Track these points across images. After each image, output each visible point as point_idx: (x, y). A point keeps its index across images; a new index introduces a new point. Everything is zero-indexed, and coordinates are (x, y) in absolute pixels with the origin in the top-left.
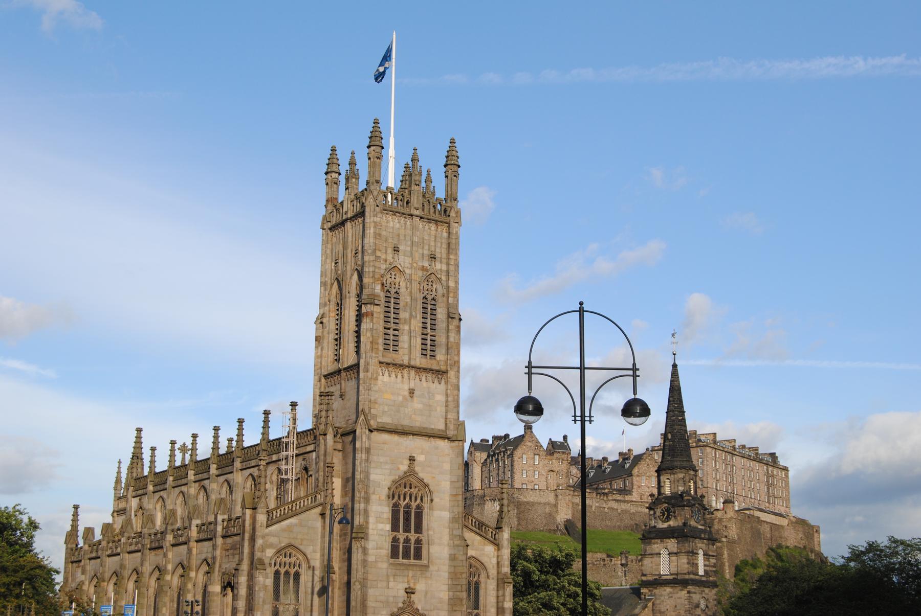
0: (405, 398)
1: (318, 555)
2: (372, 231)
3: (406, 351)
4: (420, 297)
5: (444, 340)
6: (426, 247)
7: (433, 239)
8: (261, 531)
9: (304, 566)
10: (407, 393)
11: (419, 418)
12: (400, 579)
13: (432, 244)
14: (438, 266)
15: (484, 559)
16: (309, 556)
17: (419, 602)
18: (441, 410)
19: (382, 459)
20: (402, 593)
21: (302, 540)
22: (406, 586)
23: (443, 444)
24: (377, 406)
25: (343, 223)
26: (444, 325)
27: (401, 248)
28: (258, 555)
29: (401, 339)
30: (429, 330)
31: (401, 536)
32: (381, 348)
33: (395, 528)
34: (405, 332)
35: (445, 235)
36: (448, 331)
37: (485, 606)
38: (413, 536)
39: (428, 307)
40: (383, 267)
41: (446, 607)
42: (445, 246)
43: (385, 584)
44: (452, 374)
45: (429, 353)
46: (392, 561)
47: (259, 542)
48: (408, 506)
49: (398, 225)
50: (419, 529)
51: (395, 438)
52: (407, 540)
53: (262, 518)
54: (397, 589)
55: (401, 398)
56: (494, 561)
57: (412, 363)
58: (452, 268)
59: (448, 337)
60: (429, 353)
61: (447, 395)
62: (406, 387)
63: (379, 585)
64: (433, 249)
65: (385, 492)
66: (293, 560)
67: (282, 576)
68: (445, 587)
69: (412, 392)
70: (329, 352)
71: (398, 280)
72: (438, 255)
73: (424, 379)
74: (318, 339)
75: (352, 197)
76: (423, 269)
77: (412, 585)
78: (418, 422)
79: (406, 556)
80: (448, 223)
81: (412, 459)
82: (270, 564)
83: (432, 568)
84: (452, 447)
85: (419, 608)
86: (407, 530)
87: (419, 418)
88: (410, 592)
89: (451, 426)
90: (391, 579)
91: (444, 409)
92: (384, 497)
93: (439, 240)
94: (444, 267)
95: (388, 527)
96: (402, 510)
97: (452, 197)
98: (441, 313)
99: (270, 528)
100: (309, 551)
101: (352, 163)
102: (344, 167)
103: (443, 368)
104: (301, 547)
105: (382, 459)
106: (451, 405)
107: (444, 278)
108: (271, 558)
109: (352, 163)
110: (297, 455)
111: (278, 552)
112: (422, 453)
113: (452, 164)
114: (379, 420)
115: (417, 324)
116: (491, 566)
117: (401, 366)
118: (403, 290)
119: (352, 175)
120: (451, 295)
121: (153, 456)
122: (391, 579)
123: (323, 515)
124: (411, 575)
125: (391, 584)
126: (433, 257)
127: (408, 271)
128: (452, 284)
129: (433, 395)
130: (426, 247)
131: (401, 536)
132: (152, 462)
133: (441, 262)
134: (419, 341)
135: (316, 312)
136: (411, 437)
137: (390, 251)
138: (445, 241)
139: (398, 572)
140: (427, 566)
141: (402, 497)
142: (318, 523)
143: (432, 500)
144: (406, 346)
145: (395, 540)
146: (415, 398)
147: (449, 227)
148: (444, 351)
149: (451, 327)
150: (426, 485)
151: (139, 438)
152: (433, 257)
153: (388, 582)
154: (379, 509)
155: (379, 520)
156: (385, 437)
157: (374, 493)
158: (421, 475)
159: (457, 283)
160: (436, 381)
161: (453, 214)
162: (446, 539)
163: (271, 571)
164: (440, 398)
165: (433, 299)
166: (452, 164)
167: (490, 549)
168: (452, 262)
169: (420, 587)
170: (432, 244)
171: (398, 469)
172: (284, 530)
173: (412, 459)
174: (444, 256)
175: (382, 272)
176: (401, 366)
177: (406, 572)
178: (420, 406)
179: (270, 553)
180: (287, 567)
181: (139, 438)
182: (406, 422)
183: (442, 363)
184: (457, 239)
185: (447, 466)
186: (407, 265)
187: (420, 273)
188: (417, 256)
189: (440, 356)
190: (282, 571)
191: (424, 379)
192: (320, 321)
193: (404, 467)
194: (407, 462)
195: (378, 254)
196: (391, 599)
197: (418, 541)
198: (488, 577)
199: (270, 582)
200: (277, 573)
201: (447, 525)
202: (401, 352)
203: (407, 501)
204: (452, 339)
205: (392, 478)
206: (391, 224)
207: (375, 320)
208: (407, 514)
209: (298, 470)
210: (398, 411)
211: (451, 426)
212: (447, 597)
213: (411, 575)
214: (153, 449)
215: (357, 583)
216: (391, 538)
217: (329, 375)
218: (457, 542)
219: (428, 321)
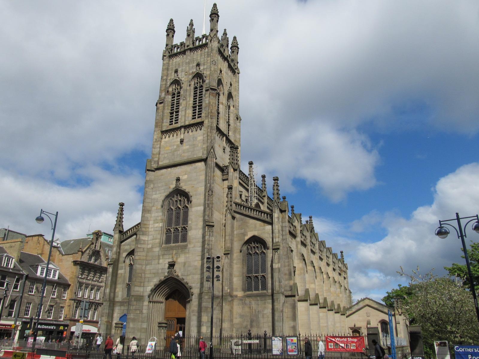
12: (166, 257)
22: (171, 260)
77: (175, 259)
81: (178, 180)
88: (172, 265)
90: (161, 257)
124: (174, 253)
125: (161, 261)
139: (166, 252)
145: (168, 231)
153: (159, 259)
171: (170, 188)
173: (178, 180)
177: (171, 252)
178: (188, 147)
182: (178, 160)
193: (173, 186)
196: (160, 271)
213: (174, 253)
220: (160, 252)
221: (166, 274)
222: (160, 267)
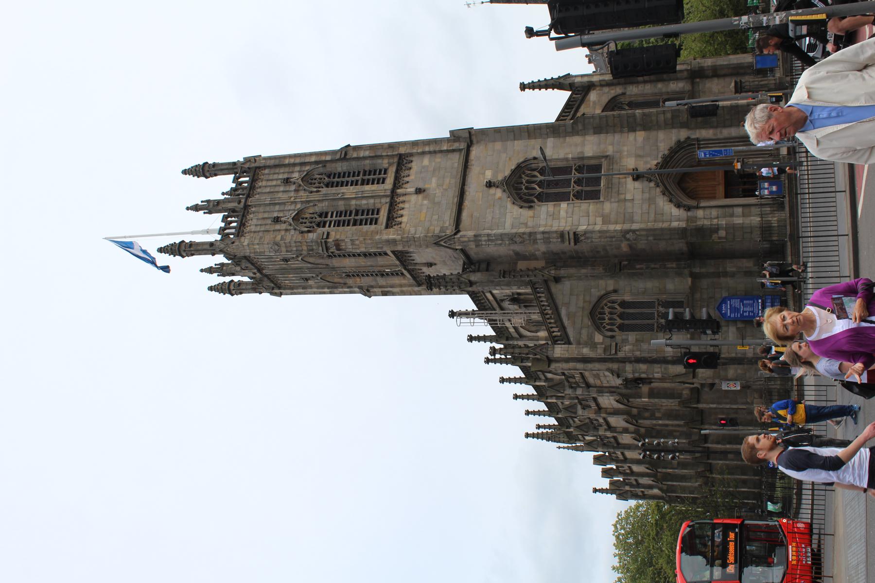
0: (425, 198)
1: (602, 283)
2: (257, 247)
3: (378, 201)
4: (324, 190)
5: (367, 162)
6: (277, 189)
7: (270, 183)
8: (572, 351)
9: (614, 297)
10: (420, 196)
11: (447, 181)
13: (274, 183)
14: (296, 175)
15: (605, 100)
16: (603, 292)
17: (651, 163)
18: (438, 158)
19: (489, 217)
20: (637, 184)
21: (585, 302)
22: (629, 179)
23: (475, 152)
24: (432, 228)
25: (266, 276)
26: (354, 163)
27: (275, 215)
28: (600, 352)
29: (365, 207)
30: (359, 178)
31: (574, 188)
32: (373, 227)
33: (564, 197)
34: (358, 202)
35: (267, 171)
36: (358, 159)
37: (655, 94)
38: (575, 175)
39: (335, 180)
40: (292, 232)
41: (653, 133)
42: (277, 171)
43: (629, 204)
44: (402, 150)
45: (382, 176)
46: (602, 199)
47: (586, 351)
48: (540, 184)
49: (255, 222)
50: (566, 170)
51: (467, 203)
52: (578, 182)
53: (559, 351)
54: (632, 188)
55: (425, 202)
56: (606, 89)
57: (389, 193)
58: (298, 161)
59: (365, 158)
60: (382, 176)
61: (423, 153)
62: (414, 198)
63: (630, 210)
64: (279, 182)
65: (526, 213)
66: (607, 310)
67: (626, 322)
68: (631, 136)
69: (419, 191)
70: (396, 280)
71: (308, 216)
72: (286, 176)
73: (406, 179)
74: (385, 294)
75: (238, 268)
76: (296, 191)
78: (451, 182)
79: (597, 181)
80: (257, 168)
81: (490, 185)
82: (612, 337)
83: (610, 150)
84: (478, 142)
85: (655, 162)
86: (567, 183)
87: (447, 181)
88: (637, 177)
89: (456, 145)
90: (622, 197)
91: (439, 155)
92: (530, 213)
93: (271, 177)
94: (297, 168)
95: (564, 205)
96: (545, 191)
98: (341, 167)
99: (572, 339)
100: (596, 293)
101: (210, 270)
102: (216, 279)
103: (396, 160)
104: (594, 300)
105: (489, 217)
106: (432, 148)
107: (307, 168)
108: (605, 336)
109: (210, 270)
110: (502, 309)
111: (598, 328)
112: (484, 174)
113: (205, 171)
114: (447, 224)
115: (349, 191)
116: (612, 92)
117: (392, 206)
118: (317, 209)
119: (220, 270)
120: (323, 158)
121: (544, 427)
122: (622, 197)
123: (557, 280)
125: (629, 197)
126: (287, 181)
127: (299, 206)
128: (313, 159)
129: (423, 167)
130: (277, 189)
131: (574, 188)
132: (549, 427)
133: (293, 172)
134: (367, 188)
135: (359, 297)
136: (466, 188)
137: (278, 227)
138: (273, 171)
139: (614, 190)
140: (606, 157)
141: (531, 192)
142: (567, 285)
143: (535, 158)
144: (372, 201)
145: (578, 196)
146: (426, 186)
147: (259, 168)
148: (379, 161)
149: (355, 155)
150: (519, 167)
151: (533, 436)
152: (287, 181)
153: (625, 200)
154: (543, 216)
155: (554, 216)
156: (465, 215)
157: (526, 224)
158: (507, 173)
159: (311, 154)
160: (409, 165)
161: (247, 166)
162: (577, 139)
163: (619, 336)
164: (426, 161)
165: (329, 177)
166: (205, 171)
167: (593, 96)
168: (292, 161)
169: (630, 163)
170: (274, 183)
171: (500, 198)
172: (574, 323)
173: (490, 185)
174: (287, 170)
175: (297, 232)
176: (392, 206)
178: (434, 180)
179: (598, 338)
180: (615, 316)
181: (533, 436)
182: (452, 196)
183: (391, 161)
184: (270, 158)
185: (498, 145)
186: (292, 207)
187: (302, 193)
188: (283, 197)
189: (385, 163)
190: (619, 321)
191: (406, 179)
192: (367, 292)
193: (498, 193)
194: (492, 191)
195: (279, 238)
196: (647, 195)
197: (580, 169)
198: (624, 94)
199: (632, 336)
200: (622, 328)
201: (562, 139)
202: (378, 206)
203: (536, 187)
204: (367, 153)
205: (509, 205)
206: (253, 228)
207: (343, 237)
208: (549, 184)
209: (516, 307)
210: (439, 203)
211: (456, 145)
212: (643, 133)
214: (539, 427)
215: (628, 236)
216: (576, 201)
217: (416, 281)
218: (580, 127)
219: (350, 179)
220: (613, 200)
221: (652, 184)
222: (638, 196)
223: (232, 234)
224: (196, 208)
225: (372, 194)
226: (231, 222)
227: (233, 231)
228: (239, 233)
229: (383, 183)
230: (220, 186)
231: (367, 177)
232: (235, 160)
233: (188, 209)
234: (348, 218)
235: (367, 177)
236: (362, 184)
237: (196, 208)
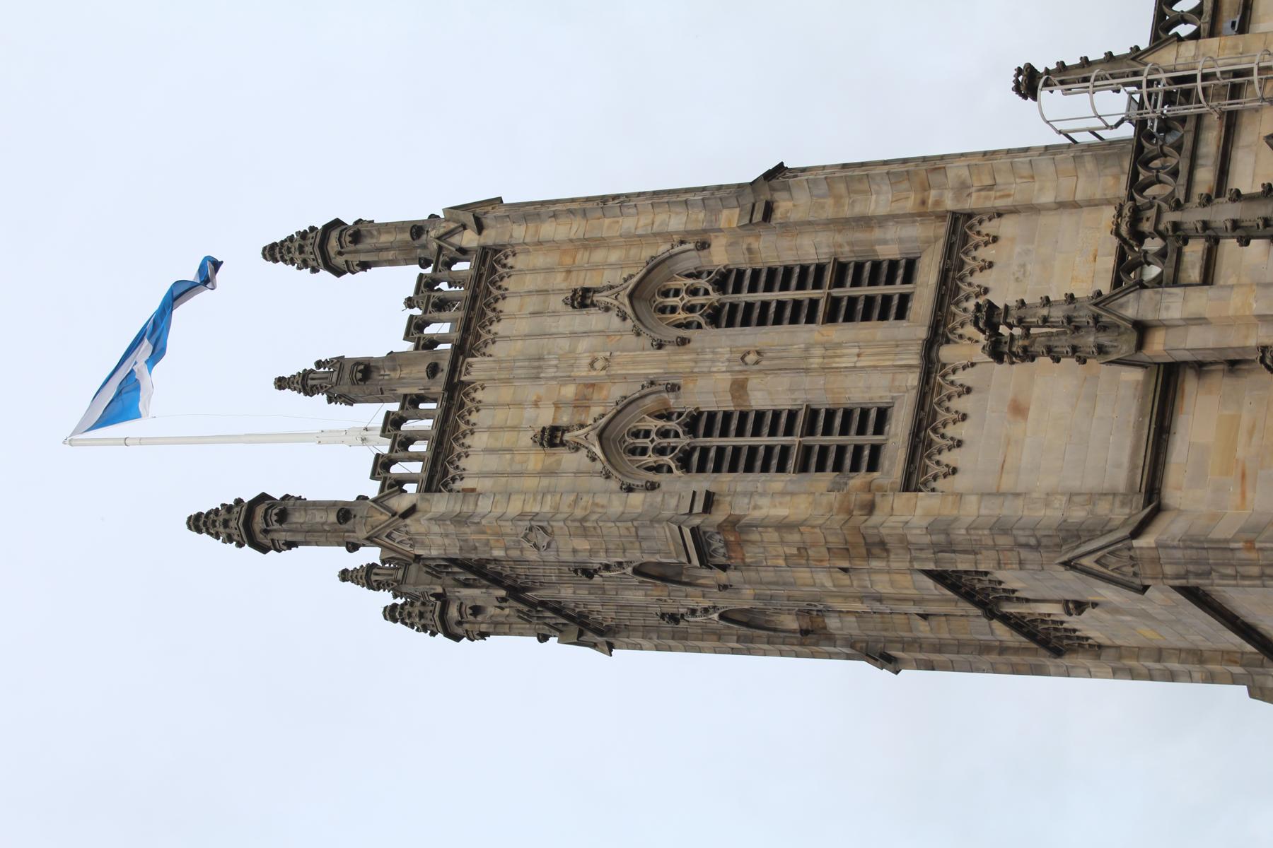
6: (549, 323)
60: (897, 289)
97: (413, 241)
103: (942, 230)
152: (582, 299)
223: (411, 479)
224: (305, 383)
225: (865, 364)
226: (409, 440)
227: (416, 467)
228: (438, 476)
229: (901, 315)
230: (372, 312)
231: (846, 292)
232: (421, 215)
233: (281, 383)
234: (780, 440)
235: (846, 292)
236: (831, 318)
237: (305, 383)
